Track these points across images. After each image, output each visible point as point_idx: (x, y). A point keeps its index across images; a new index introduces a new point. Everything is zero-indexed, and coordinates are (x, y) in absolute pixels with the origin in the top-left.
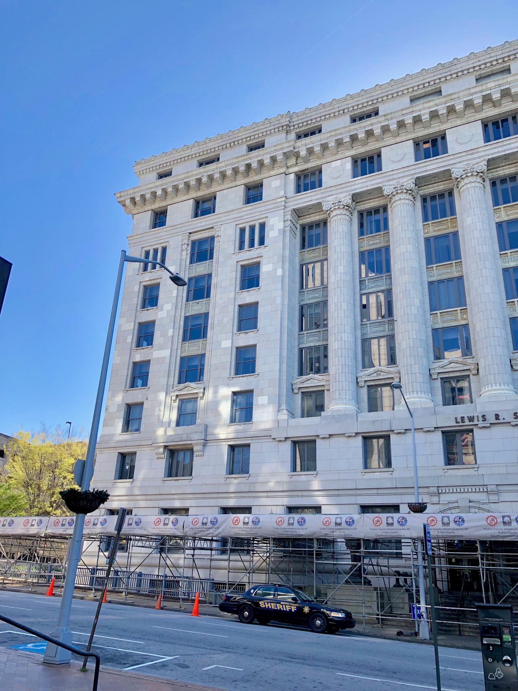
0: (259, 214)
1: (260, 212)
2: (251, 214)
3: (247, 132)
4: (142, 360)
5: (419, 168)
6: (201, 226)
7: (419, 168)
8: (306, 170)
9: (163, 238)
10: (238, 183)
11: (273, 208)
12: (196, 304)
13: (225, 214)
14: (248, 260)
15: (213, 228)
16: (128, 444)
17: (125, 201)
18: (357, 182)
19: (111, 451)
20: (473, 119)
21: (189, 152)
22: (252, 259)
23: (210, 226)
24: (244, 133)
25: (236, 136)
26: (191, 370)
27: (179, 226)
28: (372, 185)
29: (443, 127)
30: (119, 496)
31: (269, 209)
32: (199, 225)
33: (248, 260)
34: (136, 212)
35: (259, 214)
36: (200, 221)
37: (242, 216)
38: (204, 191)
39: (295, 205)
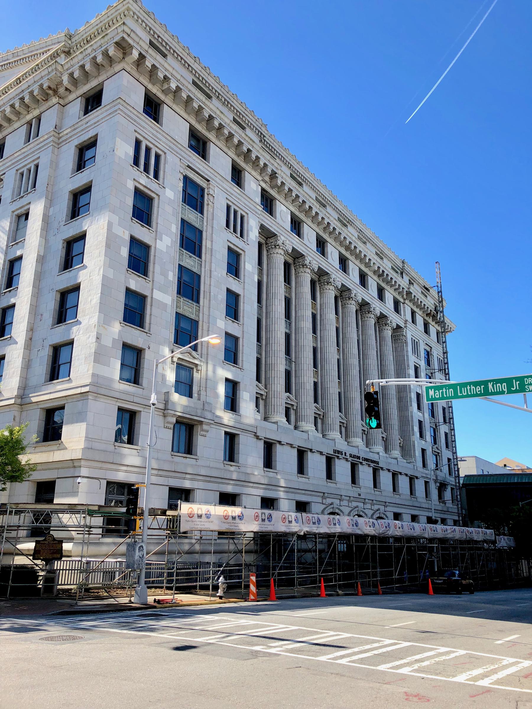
0: (243, 205)
1: (245, 204)
2: (239, 199)
3: (240, 106)
4: (138, 290)
5: (320, 259)
6: (199, 169)
7: (320, 259)
8: (267, 192)
9: (161, 143)
10: (230, 153)
11: (253, 210)
12: (188, 256)
13: (220, 178)
14: (234, 245)
15: (208, 181)
16: (136, 400)
17: (131, 47)
18: (295, 239)
19: (109, 402)
20: (337, 247)
21: (196, 66)
22: (237, 247)
23: (206, 177)
24: (238, 105)
25: (232, 99)
26: (186, 332)
27: (179, 146)
28: (301, 249)
29: (328, 239)
30: (254, 483)
31: (250, 208)
32: (198, 165)
33: (234, 245)
34: (129, 69)
35: (243, 205)
36: (199, 161)
37: (232, 194)
38: (203, 128)
39: (264, 222)
